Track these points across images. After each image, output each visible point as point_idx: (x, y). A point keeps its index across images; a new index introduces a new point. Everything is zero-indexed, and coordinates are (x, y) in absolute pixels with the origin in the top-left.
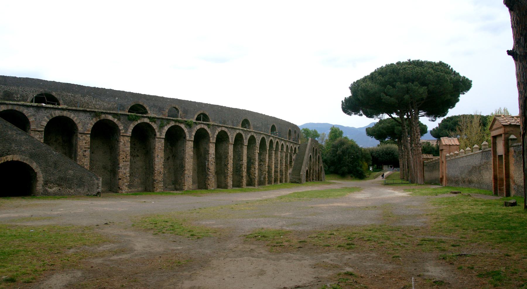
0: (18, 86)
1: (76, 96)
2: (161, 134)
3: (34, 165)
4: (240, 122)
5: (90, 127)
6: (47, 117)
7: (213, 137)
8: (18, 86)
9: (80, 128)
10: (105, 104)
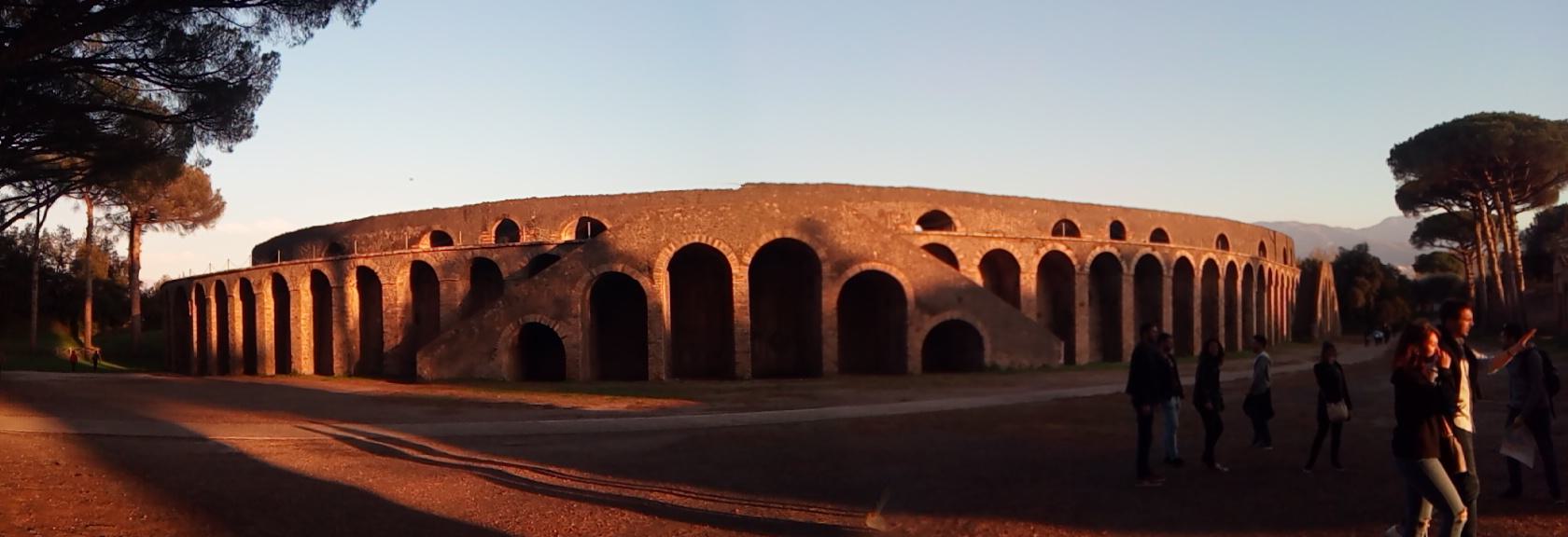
0: (897, 201)
1: (978, 212)
2: (1129, 268)
3: (979, 325)
4: (1212, 240)
5: (1036, 261)
6: (981, 252)
7: (1198, 268)
8: (897, 201)
9: (1022, 264)
10: (1019, 222)
